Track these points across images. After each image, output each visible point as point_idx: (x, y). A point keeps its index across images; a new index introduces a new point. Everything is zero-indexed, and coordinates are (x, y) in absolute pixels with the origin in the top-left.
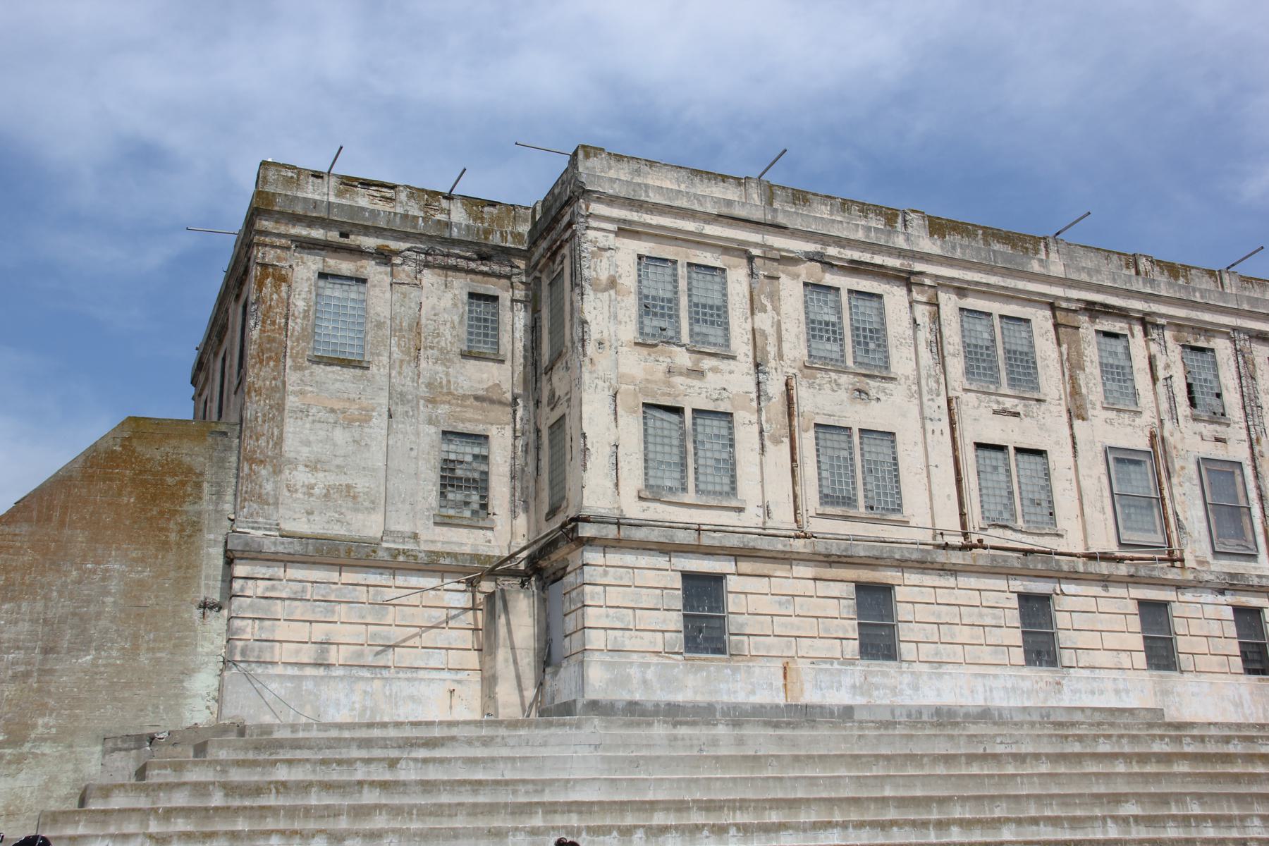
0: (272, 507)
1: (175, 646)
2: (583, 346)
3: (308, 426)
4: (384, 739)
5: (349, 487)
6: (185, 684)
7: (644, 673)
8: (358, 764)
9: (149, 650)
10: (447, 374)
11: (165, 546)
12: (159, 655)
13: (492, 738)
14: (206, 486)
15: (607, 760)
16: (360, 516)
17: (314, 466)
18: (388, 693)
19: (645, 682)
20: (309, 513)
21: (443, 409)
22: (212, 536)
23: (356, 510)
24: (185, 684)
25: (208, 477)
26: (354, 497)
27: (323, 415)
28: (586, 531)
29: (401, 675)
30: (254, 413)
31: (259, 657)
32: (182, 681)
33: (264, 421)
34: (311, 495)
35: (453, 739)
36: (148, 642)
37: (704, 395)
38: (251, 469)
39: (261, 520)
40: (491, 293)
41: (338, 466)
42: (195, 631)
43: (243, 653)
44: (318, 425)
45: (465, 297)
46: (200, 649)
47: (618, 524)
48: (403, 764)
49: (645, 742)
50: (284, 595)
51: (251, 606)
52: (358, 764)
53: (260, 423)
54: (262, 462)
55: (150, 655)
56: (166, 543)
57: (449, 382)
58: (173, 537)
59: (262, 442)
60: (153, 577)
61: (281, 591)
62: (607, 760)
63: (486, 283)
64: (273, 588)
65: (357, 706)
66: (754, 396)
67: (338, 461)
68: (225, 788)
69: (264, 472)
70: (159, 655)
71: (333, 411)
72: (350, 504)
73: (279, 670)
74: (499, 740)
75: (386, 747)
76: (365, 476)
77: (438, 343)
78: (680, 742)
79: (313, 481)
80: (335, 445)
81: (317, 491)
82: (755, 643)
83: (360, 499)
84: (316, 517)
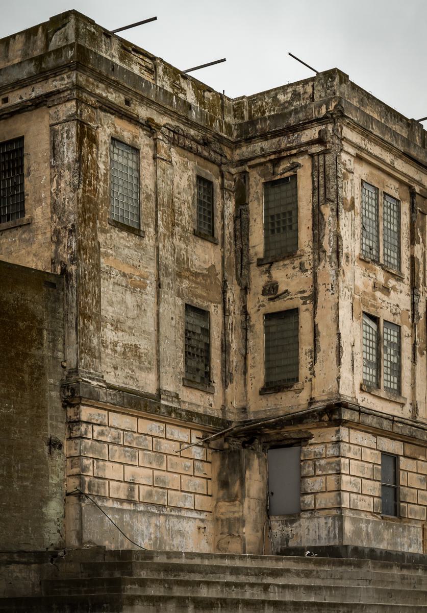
0: (97, 360)
1: (36, 476)
2: (338, 257)
3: (111, 287)
4: (247, 568)
5: (136, 346)
6: (44, 510)
7: (367, 527)
8: (247, 587)
9: (20, 478)
10: (187, 252)
11: (21, 385)
12: (25, 483)
13: (311, 572)
14: (45, 332)
15: (378, 591)
16: (144, 375)
17: (117, 325)
18: (167, 527)
19: (368, 534)
20: (116, 368)
21: (186, 284)
22: (52, 381)
23: (141, 369)
24: (44, 510)
25: (45, 325)
26: (140, 357)
27: (119, 278)
28: (347, 415)
29: (173, 513)
30: (83, 270)
31: (98, 492)
32: (41, 508)
33: (89, 279)
34: (115, 351)
35: (288, 570)
36: (17, 472)
37: (389, 309)
38: (84, 323)
39: (92, 371)
40: (208, 178)
41: (129, 328)
42: (47, 464)
43: (89, 489)
44: (117, 288)
45: (195, 180)
46: (51, 481)
47: (359, 411)
48: (271, 589)
49: (390, 580)
50: (108, 440)
51: (92, 447)
52: (247, 587)
53: (87, 280)
54: (90, 318)
55: (19, 483)
56: (22, 383)
57: (188, 259)
58: (27, 377)
59: (89, 299)
60: (16, 413)
61: (107, 436)
62: (378, 591)
63: (206, 167)
64: (101, 433)
65: (153, 536)
66: (410, 313)
67: (129, 323)
68: (194, 602)
69: (91, 328)
70: (25, 483)
71: (124, 275)
72: (138, 364)
73: (109, 504)
74: (315, 573)
75: (247, 574)
76: (145, 338)
77: (181, 220)
78: (406, 581)
79: (116, 339)
80: (127, 308)
81: (118, 349)
82: (411, 509)
83: (143, 360)
84: (119, 372)
